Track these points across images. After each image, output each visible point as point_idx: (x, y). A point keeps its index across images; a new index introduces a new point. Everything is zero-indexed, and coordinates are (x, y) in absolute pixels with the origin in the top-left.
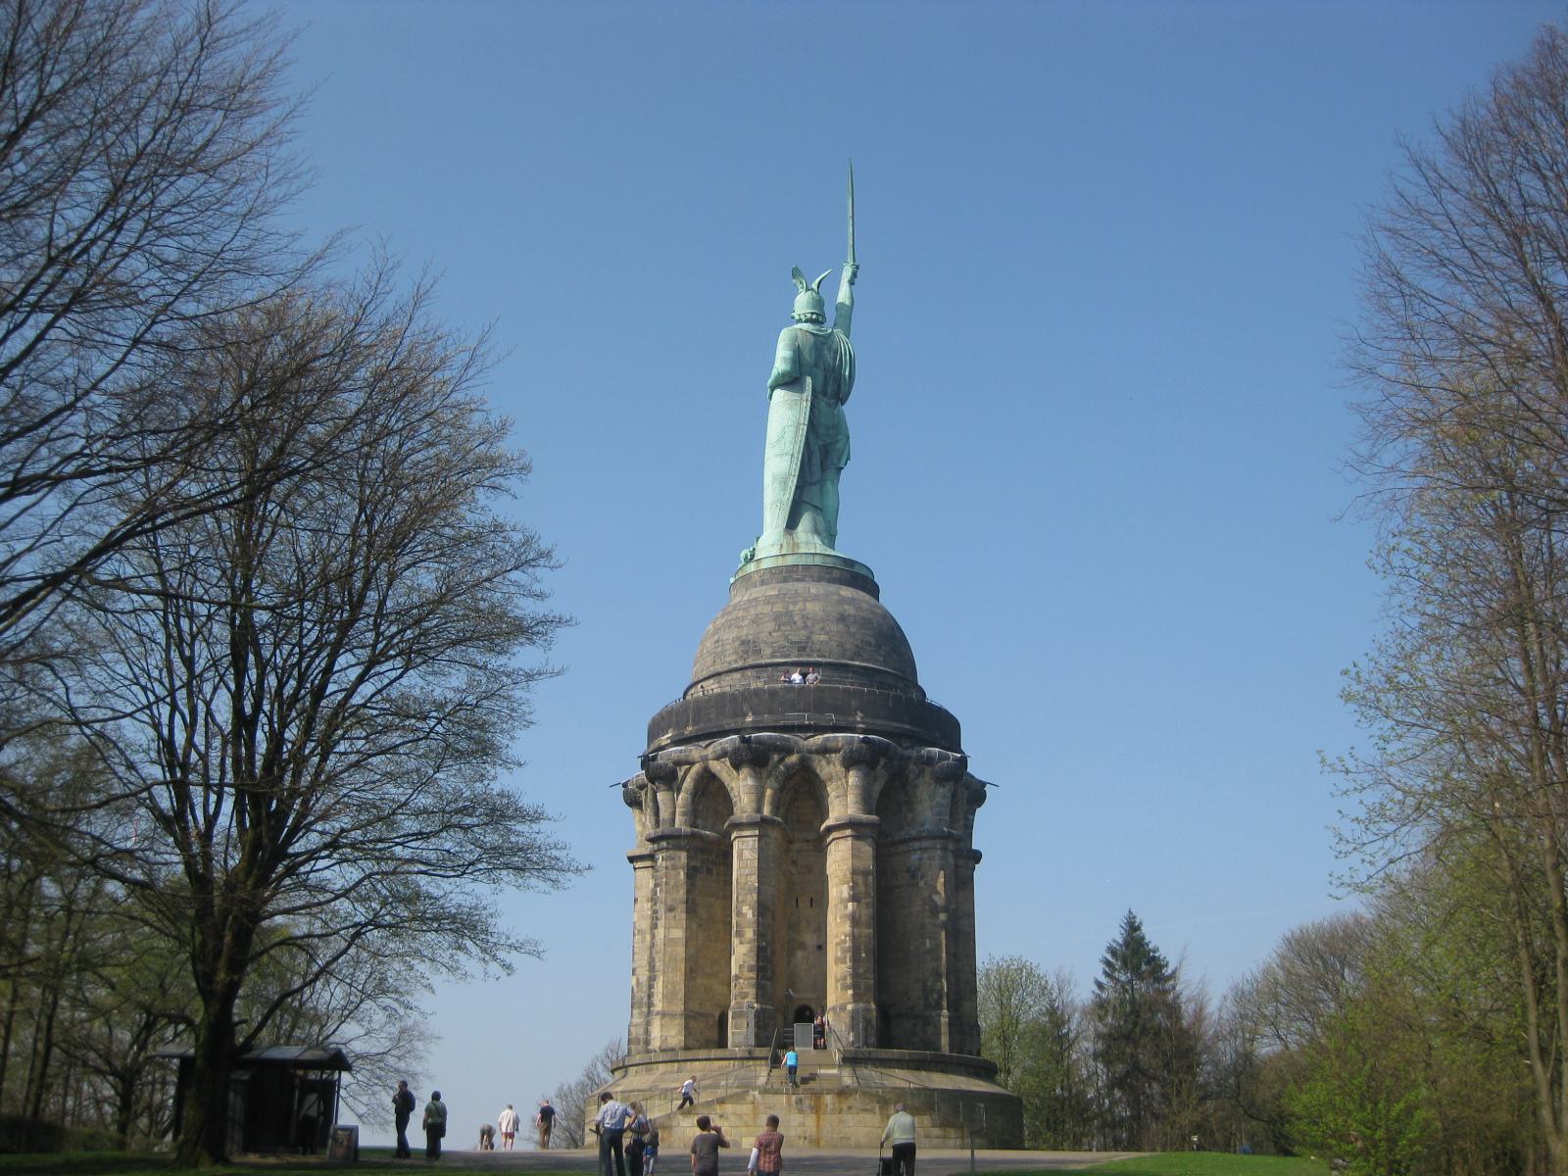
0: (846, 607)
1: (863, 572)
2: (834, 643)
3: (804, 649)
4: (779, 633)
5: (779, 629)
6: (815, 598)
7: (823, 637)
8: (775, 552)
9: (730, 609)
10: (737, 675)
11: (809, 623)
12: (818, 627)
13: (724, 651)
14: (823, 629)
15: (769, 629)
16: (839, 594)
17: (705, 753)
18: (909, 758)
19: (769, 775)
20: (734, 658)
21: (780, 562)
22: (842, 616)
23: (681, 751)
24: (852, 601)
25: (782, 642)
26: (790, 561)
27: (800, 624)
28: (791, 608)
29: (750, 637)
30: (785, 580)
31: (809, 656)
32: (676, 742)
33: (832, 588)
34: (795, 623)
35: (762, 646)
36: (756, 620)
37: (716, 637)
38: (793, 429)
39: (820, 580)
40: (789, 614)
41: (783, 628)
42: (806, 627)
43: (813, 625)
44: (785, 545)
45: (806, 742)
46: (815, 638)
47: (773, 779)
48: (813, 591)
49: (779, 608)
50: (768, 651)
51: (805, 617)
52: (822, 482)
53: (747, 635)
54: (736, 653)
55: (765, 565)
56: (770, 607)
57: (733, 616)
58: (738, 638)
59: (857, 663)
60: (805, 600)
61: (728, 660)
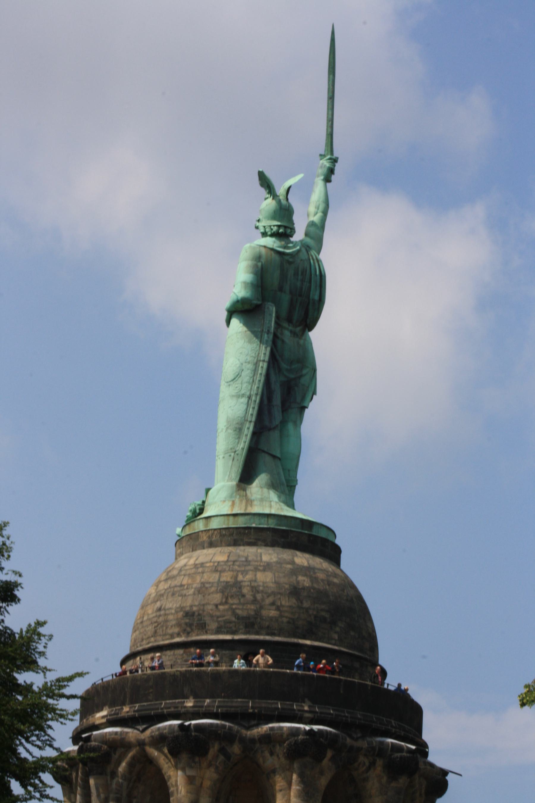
0: (300, 578)
1: (323, 534)
2: (285, 620)
3: (252, 625)
4: (226, 607)
5: (226, 603)
6: (267, 567)
7: (273, 613)
8: (226, 509)
9: (175, 572)
10: (181, 651)
11: (259, 596)
12: (268, 601)
13: (166, 621)
14: (273, 604)
15: (216, 601)
16: (293, 563)
17: (143, 736)
18: (359, 749)
19: (210, 765)
20: (176, 630)
21: (232, 523)
22: (295, 588)
23: (116, 733)
24: (308, 571)
25: (229, 616)
26: (241, 522)
27: (249, 597)
28: (240, 578)
29: (195, 609)
30: (235, 543)
31: (257, 633)
32: (111, 723)
33: (286, 554)
34: (244, 596)
35: (207, 619)
36: (202, 590)
37: (158, 604)
38: (250, 366)
39: (273, 544)
40: (237, 584)
41: (230, 601)
42: (255, 601)
43: (263, 600)
44: (237, 501)
45: (249, 733)
46: (264, 613)
47: (212, 769)
48: (265, 558)
49: (227, 577)
50: (213, 626)
51: (255, 589)
52: (284, 422)
53: (191, 606)
54: (179, 625)
55: (215, 524)
56: (217, 575)
57: (177, 582)
58: (181, 608)
59: (308, 642)
60: (256, 569)
61: (170, 631)
